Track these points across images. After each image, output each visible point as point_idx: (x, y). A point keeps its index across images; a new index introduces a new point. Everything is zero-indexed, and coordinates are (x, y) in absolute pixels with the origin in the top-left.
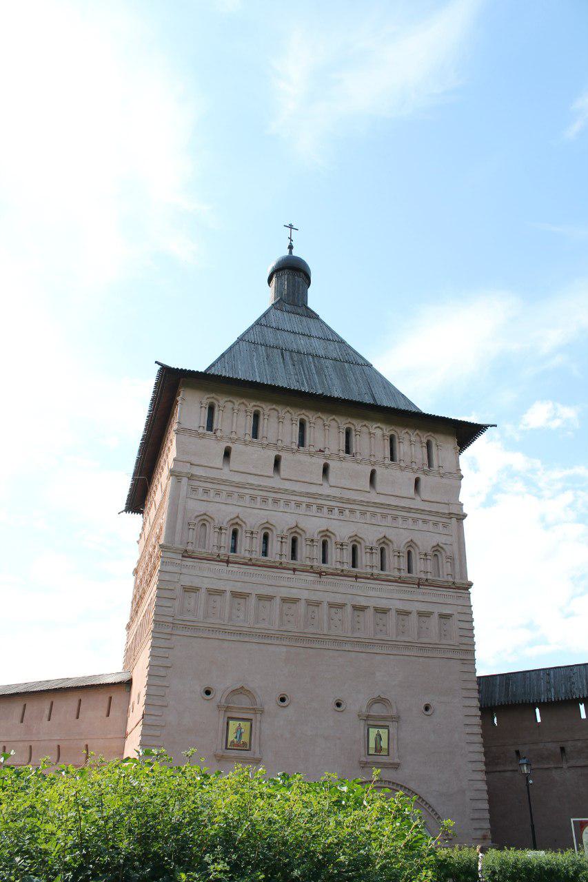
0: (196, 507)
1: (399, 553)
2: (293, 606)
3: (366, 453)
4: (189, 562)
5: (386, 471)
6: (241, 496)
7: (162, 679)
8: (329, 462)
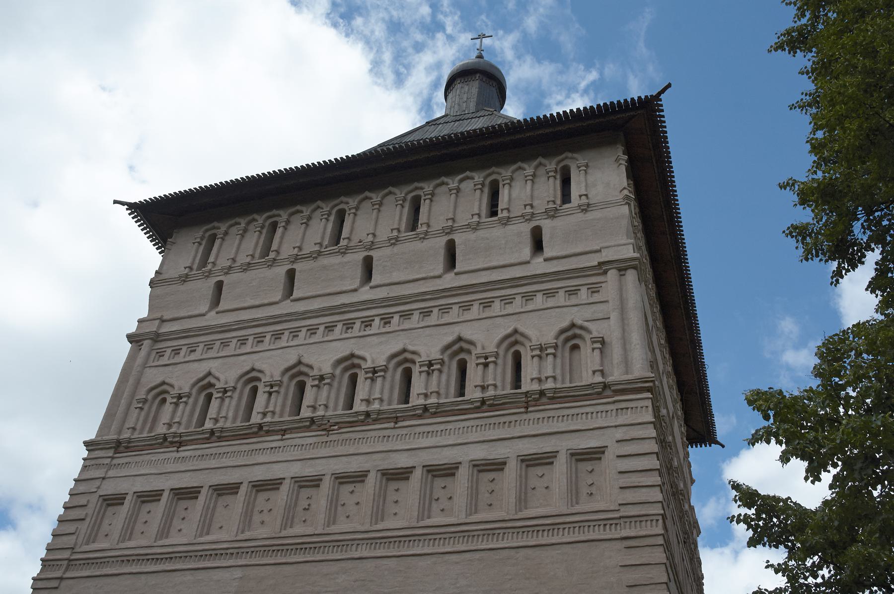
0: (153, 377)
5: (472, 236)
8: (371, 253)
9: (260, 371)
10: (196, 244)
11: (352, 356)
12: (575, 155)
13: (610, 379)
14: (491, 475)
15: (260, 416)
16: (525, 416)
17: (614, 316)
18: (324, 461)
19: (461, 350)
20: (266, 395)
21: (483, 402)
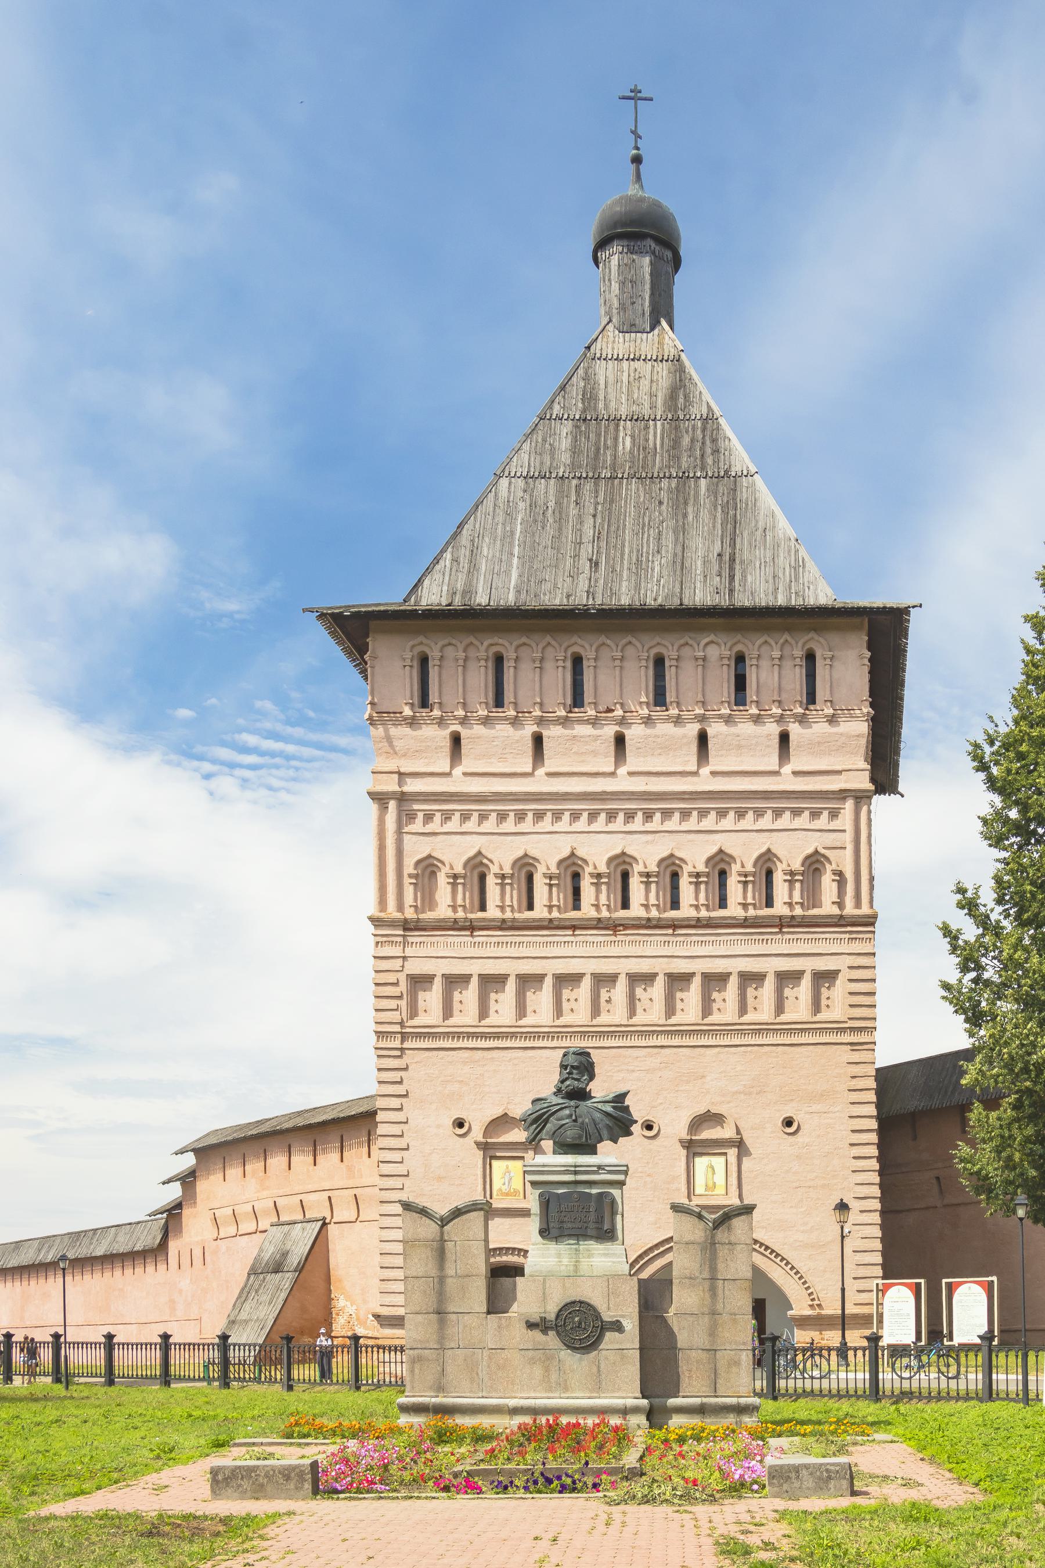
4: (415, 938)
9: (534, 859)
15: (546, 909)
17: (850, 847)
19: (722, 860)
21: (746, 919)
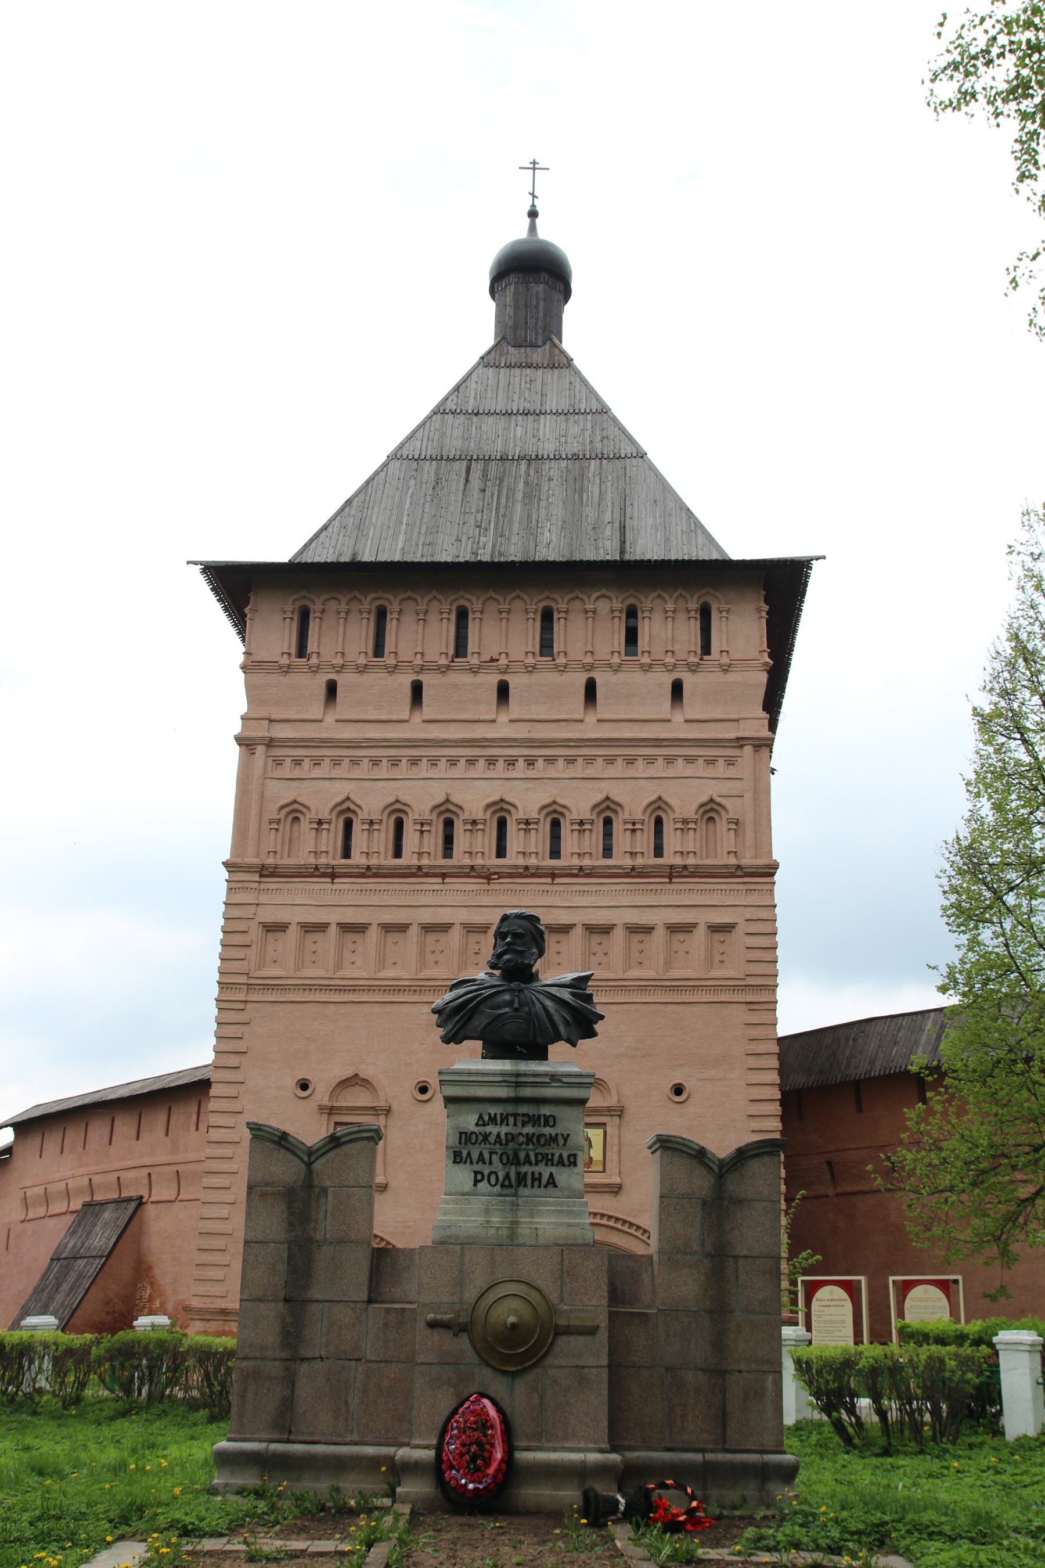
1: (634, 824)
2: (442, 937)
3: (576, 652)
4: (272, 884)
6: (355, 762)
7: (234, 1071)
8: (506, 677)
10: (288, 620)
11: (502, 800)
12: (718, 594)
13: (744, 862)
14: (640, 937)
15: (415, 856)
16: (669, 886)
17: (748, 796)
18: (489, 909)
20: (418, 834)
21: (633, 869)
